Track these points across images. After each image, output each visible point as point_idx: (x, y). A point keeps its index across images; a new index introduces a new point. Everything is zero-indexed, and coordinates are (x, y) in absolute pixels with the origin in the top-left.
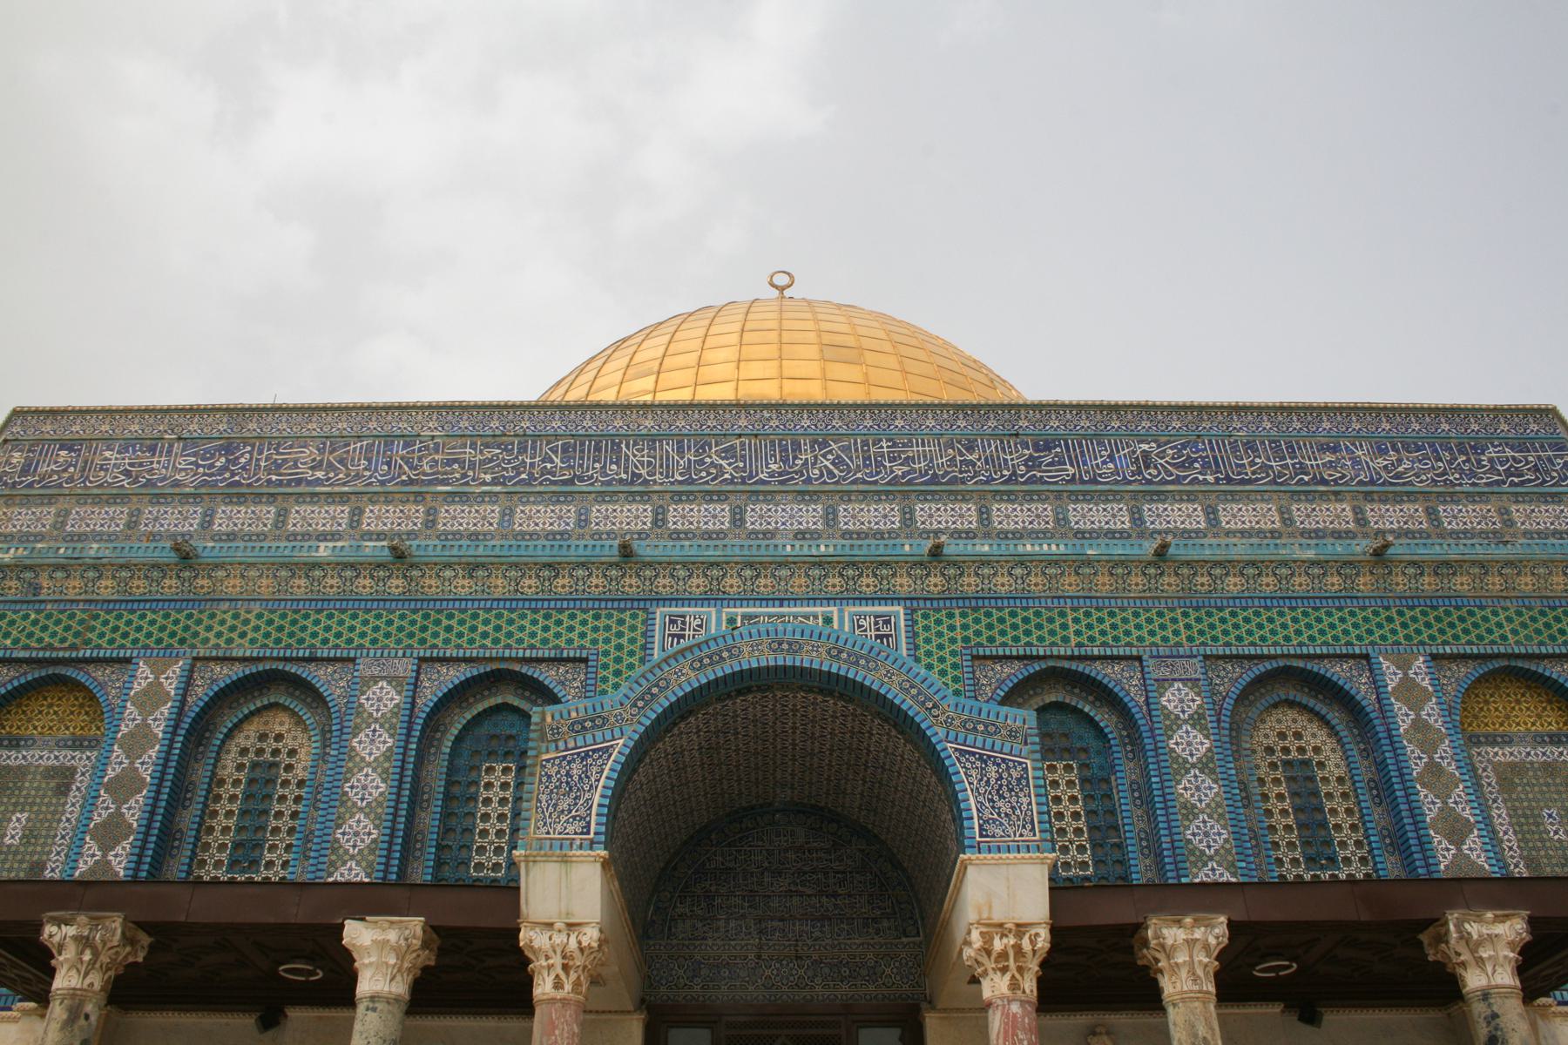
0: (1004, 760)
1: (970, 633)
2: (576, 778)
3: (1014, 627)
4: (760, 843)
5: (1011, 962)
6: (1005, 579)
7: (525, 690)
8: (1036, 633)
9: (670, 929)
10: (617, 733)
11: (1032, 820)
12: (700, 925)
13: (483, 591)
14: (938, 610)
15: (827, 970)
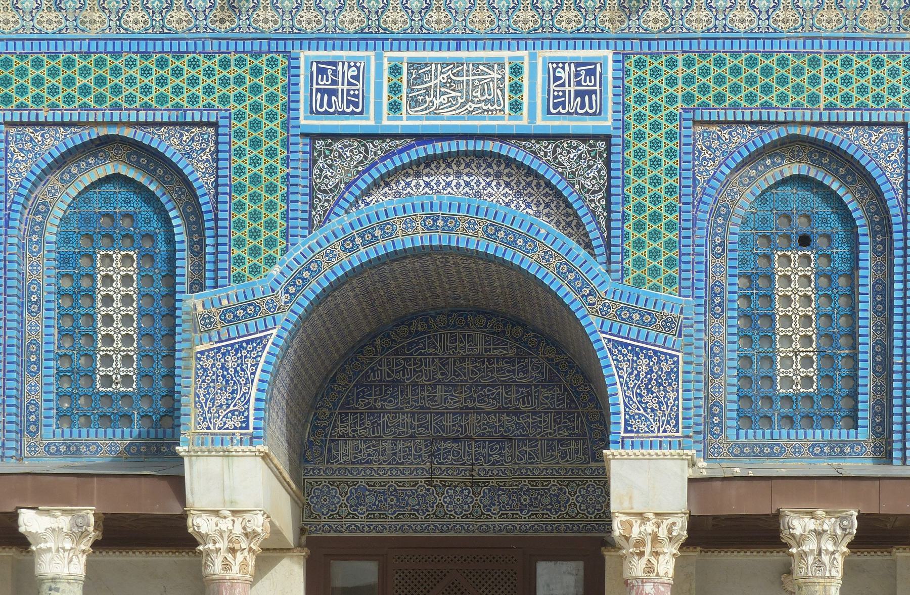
0: (655, 352)
1: (694, 89)
2: (232, 372)
3: (751, 80)
4: (432, 350)
5: (648, 549)
6: (745, 14)
7: (140, 156)
8: (778, 90)
9: (330, 451)
10: (270, 324)
11: (677, 415)
12: (363, 446)
13: (76, 28)
14: (656, 56)
15: (505, 498)
